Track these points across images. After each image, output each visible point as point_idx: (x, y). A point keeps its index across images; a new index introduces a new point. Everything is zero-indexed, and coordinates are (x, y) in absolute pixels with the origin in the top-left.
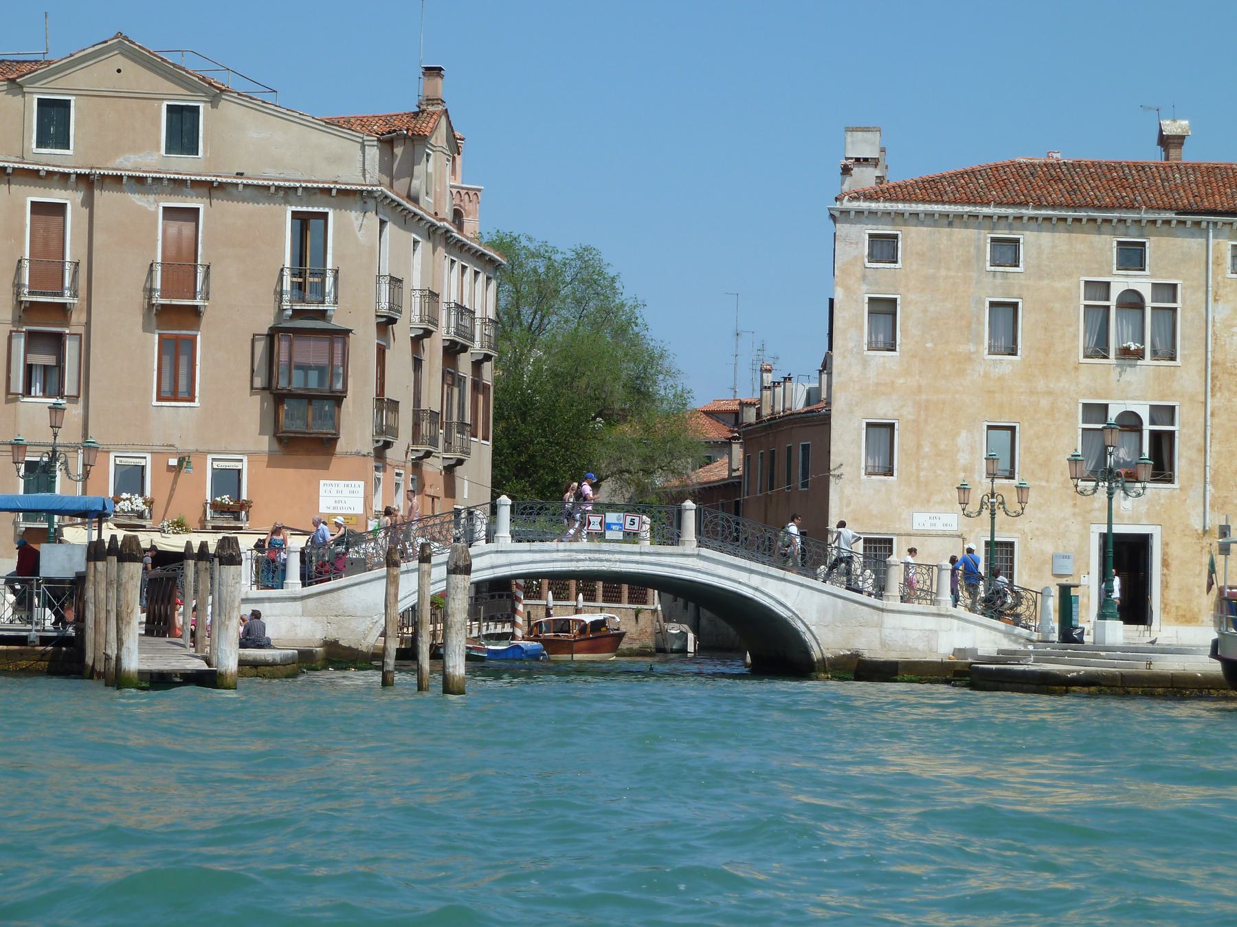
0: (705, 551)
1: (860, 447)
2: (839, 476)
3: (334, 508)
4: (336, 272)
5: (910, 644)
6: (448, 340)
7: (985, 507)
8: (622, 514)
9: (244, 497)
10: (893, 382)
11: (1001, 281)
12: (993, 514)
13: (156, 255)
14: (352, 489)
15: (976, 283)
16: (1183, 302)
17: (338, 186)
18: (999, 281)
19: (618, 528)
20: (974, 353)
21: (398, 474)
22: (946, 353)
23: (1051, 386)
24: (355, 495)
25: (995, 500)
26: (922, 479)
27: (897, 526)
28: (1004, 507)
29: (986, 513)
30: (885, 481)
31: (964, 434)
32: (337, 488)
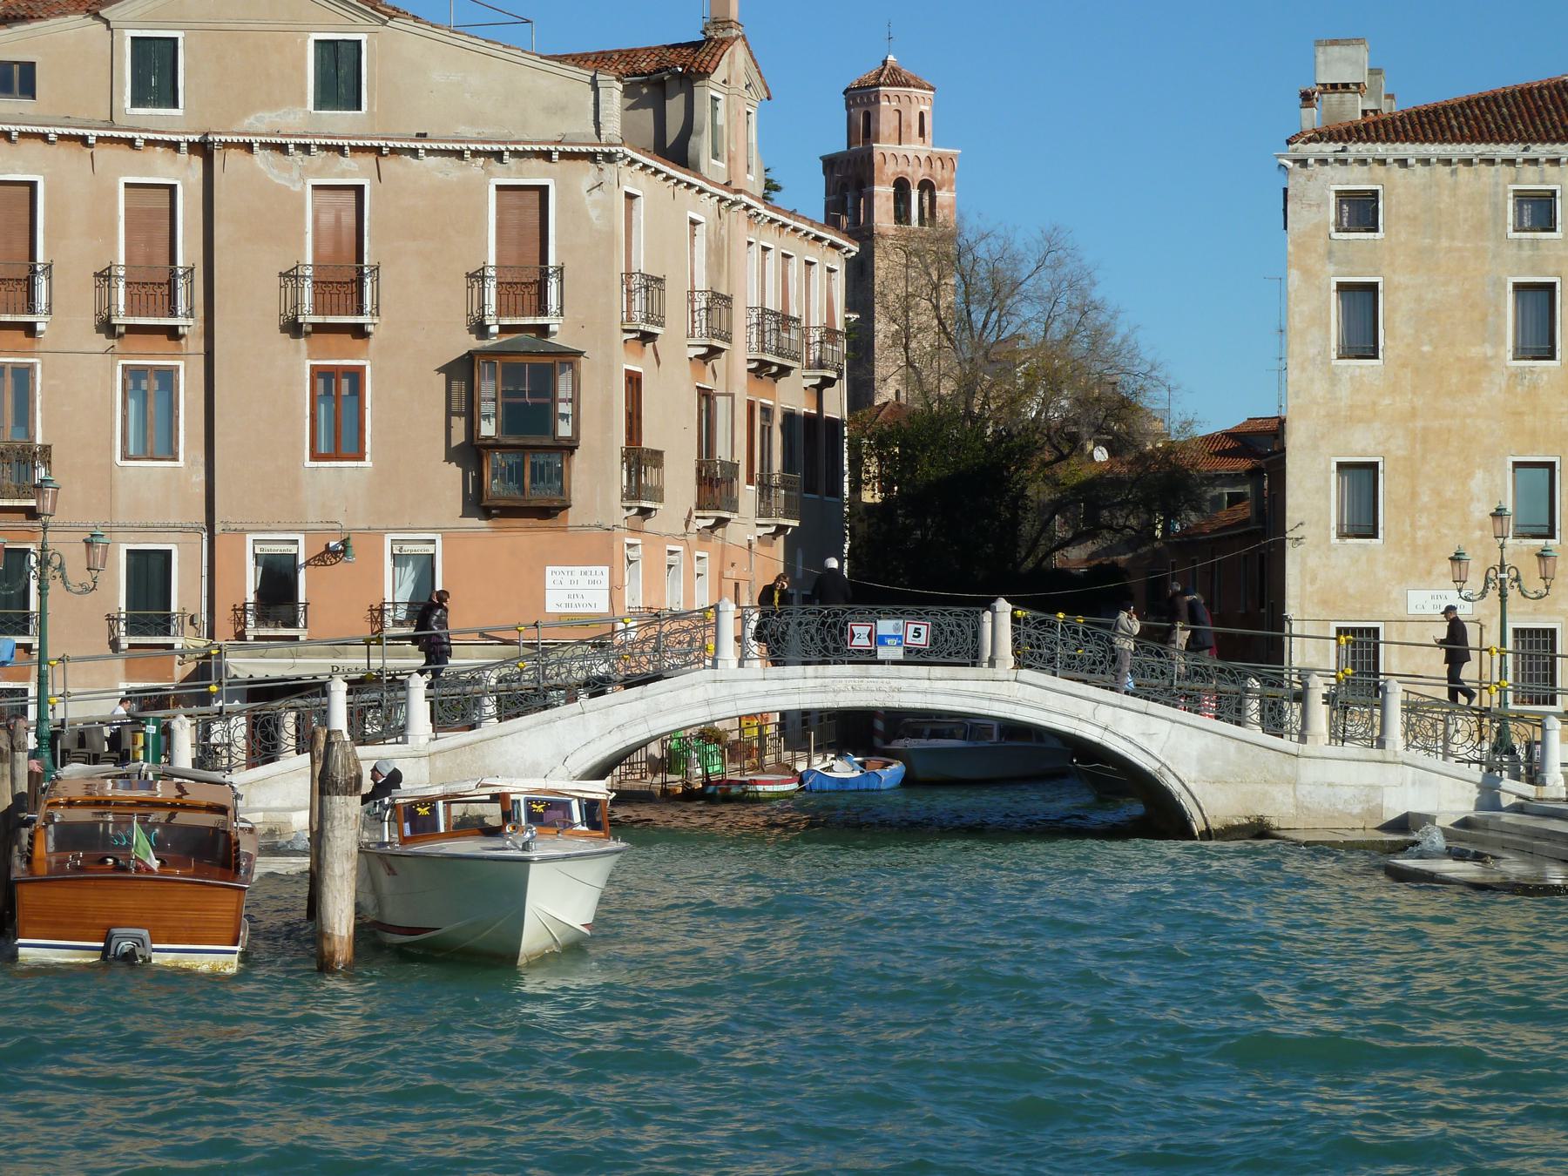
0: (1025, 674)
1: (1328, 498)
3: (567, 605)
4: (560, 270)
5: (1340, 807)
6: (755, 360)
7: (1491, 585)
8: (901, 622)
9: (439, 587)
10: (1374, 403)
11: (1530, 253)
12: (1503, 596)
13: (303, 255)
14: (592, 578)
15: (1494, 257)
17: (561, 148)
18: (1526, 253)
19: (896, 641)
20: (1491, 358)
21: (671, 553)
22: (1451, 360)
24: (596, 586)
25: (1505, 576)
26: (1420, 542)
27: (1385, 610)
28: (1519, 586)
29: (1493, 595)
30: (1366, 545)
31: (1479, 474)
32: (571, 577)
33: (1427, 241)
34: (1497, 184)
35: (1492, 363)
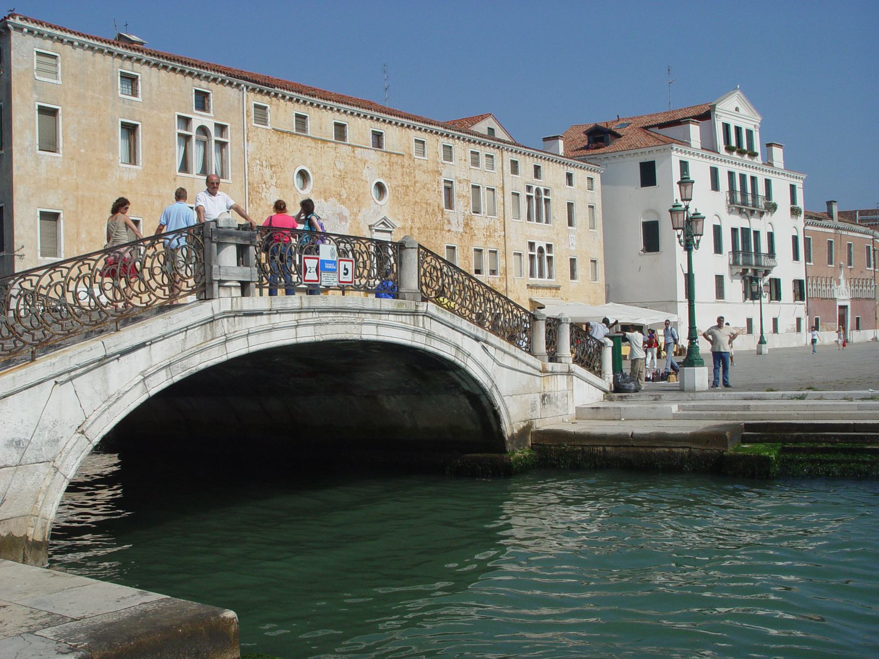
1: (36, 232)
2: (21, 256)
33: (82, 90)
35: (112, 163)
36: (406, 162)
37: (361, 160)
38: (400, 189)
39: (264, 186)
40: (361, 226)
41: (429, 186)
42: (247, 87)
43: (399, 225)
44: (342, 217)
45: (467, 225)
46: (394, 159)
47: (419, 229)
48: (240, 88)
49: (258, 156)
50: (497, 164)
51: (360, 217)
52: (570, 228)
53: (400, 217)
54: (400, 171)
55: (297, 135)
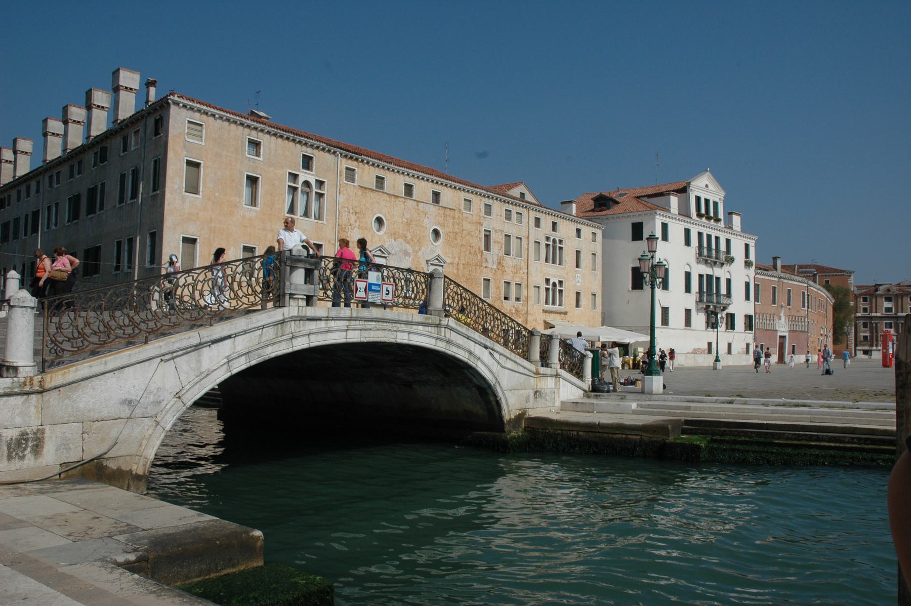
10: (197, 214)
16: (327, 191)
23: (273, 227)
34: (243, 134)
36: (457, 215)
37: (423, 212)
38: (451, 235)
39: (350, 227)
40: (420, 260)
41: (473, 233)
42: (341, 154)
43: (448, 261)
44: (406, 253)
45: (499, 263)
46: (448, 212)
47: (463, 265)
48: (336, 155)
49: (347, 205)
50: (525, 220)
51: (420, 254)
52: (577, 269)
53: (450, 255)
54: (451, 221)
55: (376, 191)
